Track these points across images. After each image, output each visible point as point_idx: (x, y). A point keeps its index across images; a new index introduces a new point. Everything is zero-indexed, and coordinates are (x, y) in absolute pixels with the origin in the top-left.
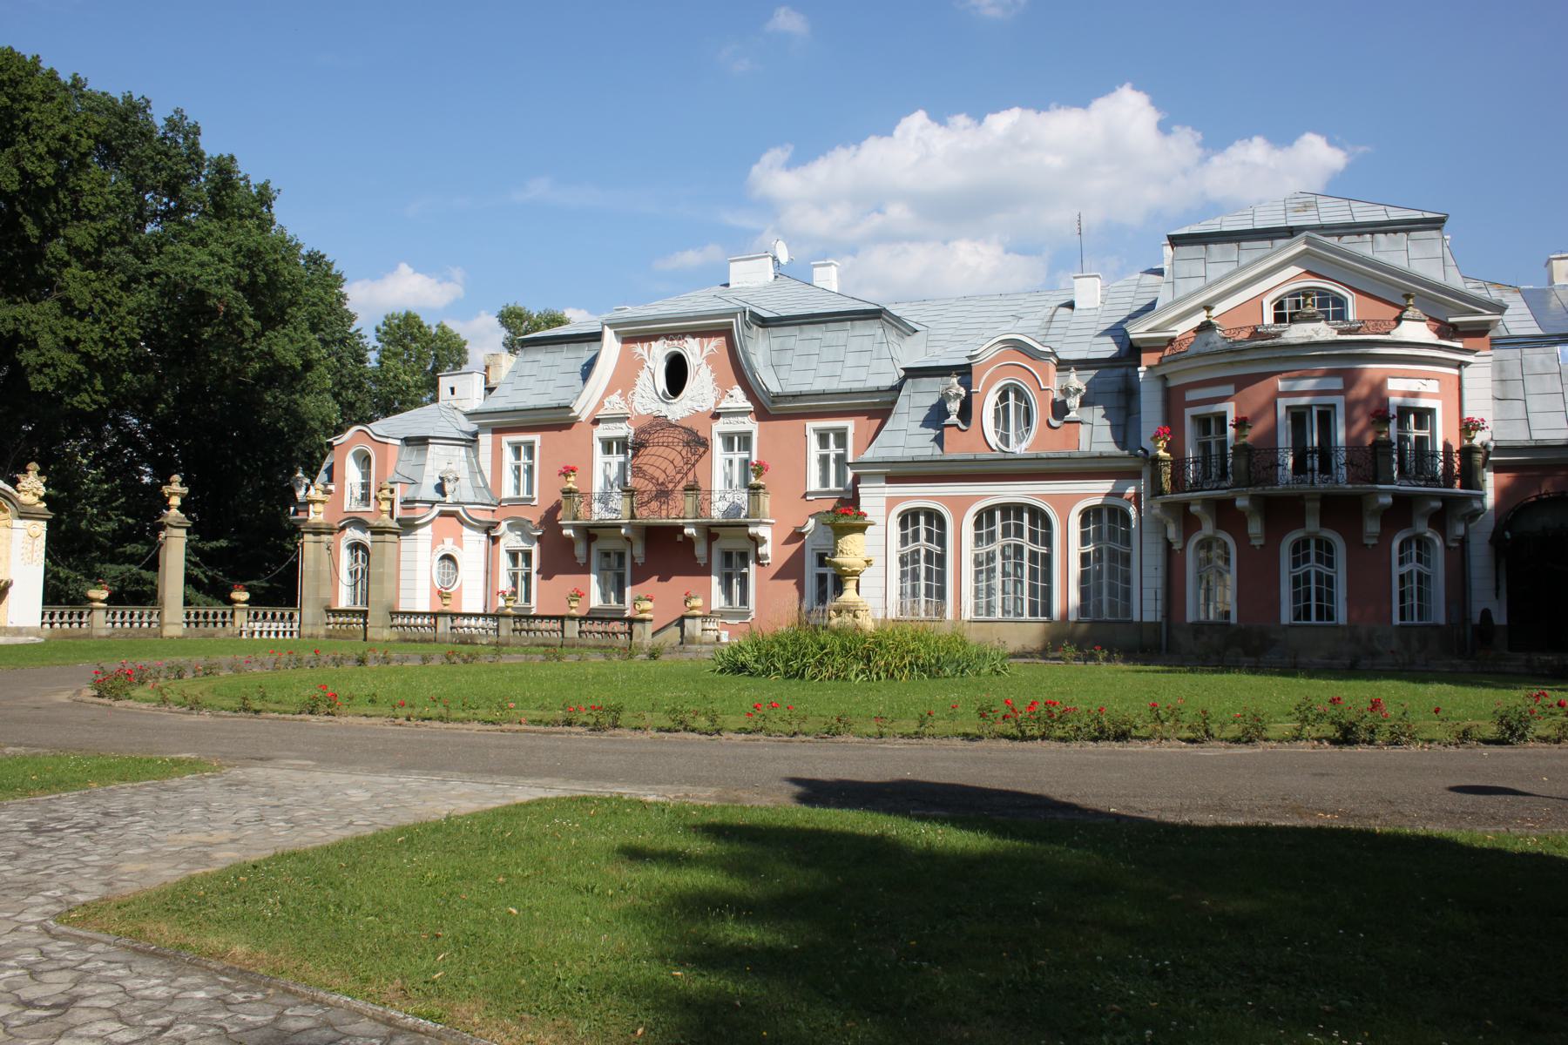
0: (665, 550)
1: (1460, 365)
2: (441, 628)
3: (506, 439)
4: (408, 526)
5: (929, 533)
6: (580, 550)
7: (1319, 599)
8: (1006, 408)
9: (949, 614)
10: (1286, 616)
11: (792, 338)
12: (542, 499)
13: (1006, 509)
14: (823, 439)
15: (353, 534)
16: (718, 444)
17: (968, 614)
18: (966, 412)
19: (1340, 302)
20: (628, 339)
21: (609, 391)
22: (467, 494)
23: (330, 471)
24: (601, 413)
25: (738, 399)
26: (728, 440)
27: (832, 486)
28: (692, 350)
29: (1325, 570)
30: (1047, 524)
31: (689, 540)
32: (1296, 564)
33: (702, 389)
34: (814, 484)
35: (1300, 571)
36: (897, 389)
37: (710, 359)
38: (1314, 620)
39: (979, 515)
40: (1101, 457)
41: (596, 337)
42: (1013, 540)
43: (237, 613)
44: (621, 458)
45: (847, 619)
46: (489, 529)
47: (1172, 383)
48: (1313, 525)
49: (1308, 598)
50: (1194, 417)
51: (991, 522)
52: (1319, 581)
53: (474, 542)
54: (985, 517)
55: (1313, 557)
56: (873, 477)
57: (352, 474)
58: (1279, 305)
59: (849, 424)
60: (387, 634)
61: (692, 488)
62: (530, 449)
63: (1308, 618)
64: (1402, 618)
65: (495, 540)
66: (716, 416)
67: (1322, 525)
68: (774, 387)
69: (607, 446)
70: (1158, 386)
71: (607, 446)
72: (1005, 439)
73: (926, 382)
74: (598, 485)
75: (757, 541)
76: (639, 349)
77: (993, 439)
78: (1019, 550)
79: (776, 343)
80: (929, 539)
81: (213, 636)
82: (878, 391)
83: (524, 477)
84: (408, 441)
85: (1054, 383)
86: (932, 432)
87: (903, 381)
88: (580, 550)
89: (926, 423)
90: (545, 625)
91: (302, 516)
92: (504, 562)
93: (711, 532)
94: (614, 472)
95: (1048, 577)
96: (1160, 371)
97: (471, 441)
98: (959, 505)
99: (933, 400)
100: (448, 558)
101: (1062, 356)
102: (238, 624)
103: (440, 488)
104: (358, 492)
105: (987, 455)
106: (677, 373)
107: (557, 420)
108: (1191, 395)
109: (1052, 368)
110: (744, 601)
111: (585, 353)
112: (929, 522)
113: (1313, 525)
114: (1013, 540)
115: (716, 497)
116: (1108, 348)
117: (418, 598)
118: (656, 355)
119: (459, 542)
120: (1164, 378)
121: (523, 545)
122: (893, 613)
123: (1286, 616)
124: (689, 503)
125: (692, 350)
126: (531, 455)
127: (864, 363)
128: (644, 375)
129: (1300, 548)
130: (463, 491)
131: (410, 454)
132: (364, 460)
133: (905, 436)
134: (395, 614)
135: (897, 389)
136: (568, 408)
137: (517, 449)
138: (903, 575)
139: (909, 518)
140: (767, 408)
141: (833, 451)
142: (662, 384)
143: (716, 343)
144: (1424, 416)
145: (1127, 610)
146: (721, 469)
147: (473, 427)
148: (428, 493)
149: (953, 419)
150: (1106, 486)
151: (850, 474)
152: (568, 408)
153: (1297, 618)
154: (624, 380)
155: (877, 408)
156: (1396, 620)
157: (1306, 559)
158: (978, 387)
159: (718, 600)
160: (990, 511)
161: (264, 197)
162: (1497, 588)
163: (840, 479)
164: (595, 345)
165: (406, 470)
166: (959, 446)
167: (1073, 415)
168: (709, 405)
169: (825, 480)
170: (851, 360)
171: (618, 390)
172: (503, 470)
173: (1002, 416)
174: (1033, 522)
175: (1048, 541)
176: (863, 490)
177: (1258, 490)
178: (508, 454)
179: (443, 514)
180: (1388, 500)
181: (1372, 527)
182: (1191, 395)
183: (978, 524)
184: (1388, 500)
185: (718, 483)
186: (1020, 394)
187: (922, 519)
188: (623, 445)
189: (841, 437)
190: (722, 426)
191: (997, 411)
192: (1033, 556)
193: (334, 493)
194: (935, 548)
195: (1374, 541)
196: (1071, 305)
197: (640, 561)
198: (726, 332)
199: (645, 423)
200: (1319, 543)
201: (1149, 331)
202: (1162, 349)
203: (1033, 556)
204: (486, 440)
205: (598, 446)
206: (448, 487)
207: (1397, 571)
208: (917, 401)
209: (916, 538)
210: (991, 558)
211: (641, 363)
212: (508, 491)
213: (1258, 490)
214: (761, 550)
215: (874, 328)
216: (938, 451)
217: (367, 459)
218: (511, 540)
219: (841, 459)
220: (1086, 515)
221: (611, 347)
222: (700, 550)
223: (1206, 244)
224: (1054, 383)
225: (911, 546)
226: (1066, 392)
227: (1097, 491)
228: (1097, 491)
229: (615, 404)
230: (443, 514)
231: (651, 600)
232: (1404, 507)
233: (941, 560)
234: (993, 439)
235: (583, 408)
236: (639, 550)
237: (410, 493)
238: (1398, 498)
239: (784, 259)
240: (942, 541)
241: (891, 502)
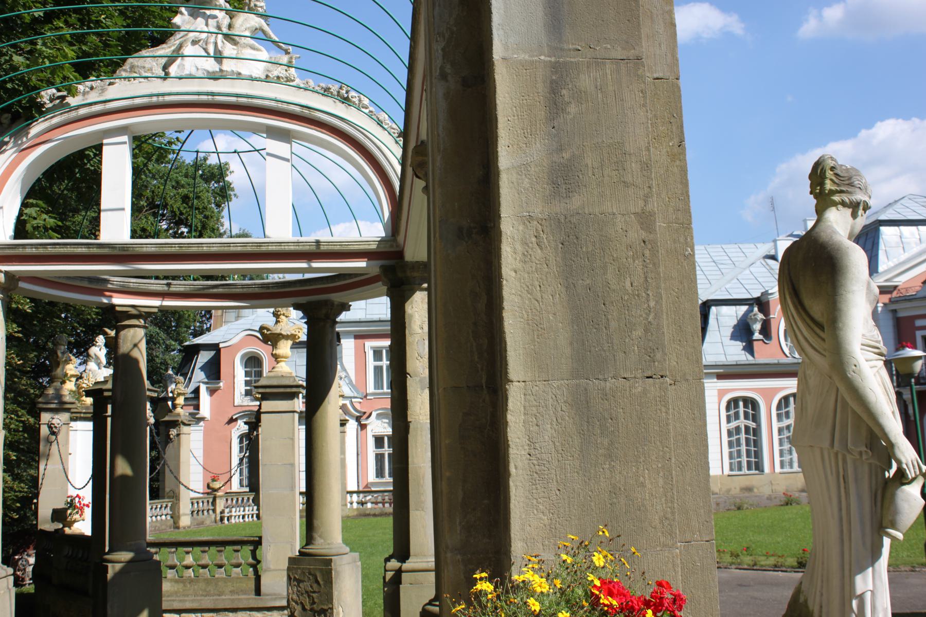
3: (370, 344)
9: (767, 468)
17: (778, 469)
18: (766, 331)
39: (780, 401)
43: (218, 501)
47: (901, 314)
56: (709, 375)
70: (890, 315)
73: (725, 309)
80: (746, 417)
81: (202, 523)
86: (739, 345)
89: (734, 337)
95: (757, 443)
96: (894, 307)
98: (768, 394)
102: (218, 510)
105: (784, 360)
120: (894, 312)
138: (730, 444)
149: (757, 336)
160: (786, 399)
182: (919, 323)
187: (741, 404)
194: (752, 425)
201: (886, 281)
202: (890, 292)
209: (737, 416)
216: (750, 357)
223: (898, 225)
225: (734, 424)
233: (757, 432)
241: (722, 393)
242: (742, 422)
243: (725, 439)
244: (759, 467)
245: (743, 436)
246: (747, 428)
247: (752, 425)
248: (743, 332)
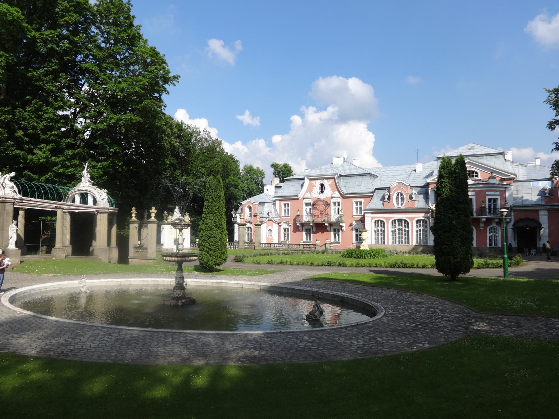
0: (320, 228)
1: (505, 188)
3: (283, 203)
4: (262, 223)
6: (300, 228)
8: (398, 198)
11: (349, 179)
12: (291, 217)
13: (398, 220)
14: (356, 203)
15: (248, 225)
16: (332, 204)
18: (389, 198)
19: (477, 173)
20: (311, 180)
21: (306, 192)
22: (274, 216)
23: (242, 209)
24: (305, 197)
25: (337, 194)
26: (334, 203)
27: (359, 214)
28: (325, 182)
30: (408, 223)
31: (326, 226)
33: (328, 192)
34: (354, 213)
36: (373, 192)
37: (330, 185)
40: (420, 209)
41: (303, 179)
42: (400, 227)
44: (310, 207)
46: (279, 223)
51: (395, 223)
53: (276, 226)
54: (394, 222)
57: (247, 210)
59: (362, 200)
60: (259, 248)
61: (327, 215)
62: (288, 205)
64: (490, 245)
65: (280, 226)
66: (332, 198)
68: (345, 192)
69: (306, 204)
71: (306, 204)
72: (398, 204)
74: (304, 214)
75: (342, 227)
76: (313, 182)
77: (396, 205)
78: (401, 229)
79: (345, 181)
82: (369, 193)
83: (287, 211)
84: (259, 203)
85: (410, 191)
86: (382, 202)
87: (375, 190)
88: (300, 228)
90: (295, 246)
91: (235, 220)
92: (283, 231)
93: (331, 224)
94: (308, 211)
97: (274, 203)
98: (388, 219)
99: (381, 195)
100: (270, 230)
101: (411, 185)
103: (268, 214)
104: (249, 215)
106: (322, 188)
107: (294, 198)
109: (409, 188)
110: (339, 240)
111: (301, 182)
112: (381, 223)
114: (400, 227)
115: (332, 217)
116: (423, 184)
117: (264, 240)
118: (318, 183)
119: (272, 227)
121: (287, 227)
122: (373, 243)
124: (326, 218)
125: (325, 182)
126: (288, 206)
127: (366, 186)
128: (315, 188)
130: (273, 215)
131: (260, 207)
132: (250, 208)
133: (376, 203)
134: (260, 244)
135: (373, 192)
136: (297, 196)
137: (285, 205)
139: (376, 222)
140: (343, 196)
141: (359, 206)
142: (319, 191)
143: (331, 181)
144: (495, 200)
145: (427, 243)
146: (333, 209)
147: (274, 199)
148: (265, 215)
149: (386, 200)
150: (423, 215)
151: (363, 212)
152: (297, 196)
154: (310, 189)
155: (370, 196)
156: (488, 246)
158: (392, 193)
159: (333, 239)
160: (395, 221)
162: (514, 239)
163: (361, 213)
164: (303, 181)
165: (259, 210)
166: (388, 206)
167: (414, 199)
168: (330, 195)
170: (363, 185)
171: (309, 192)
172: (281, 208)
173: (397, 199)
174: (405, 223)
175: (408, 227)
176: (366, 215)
178: (283, 206)
179: (269, 220)
180: (485, 220)
181: (482, 225)
183: (392, 223)
184: (485, 220)
185: (332, 213)
186: (402, 195)
188: (310, 204)
189: (361, 203)
190: (333, 200)
192: (405, 231)
193: (242, 216)
194: (383, 229)
196: (415, 171)
198: (334, 178)
199: (315, 200)
203: (405, 231)
204: (277, 202)
205: (304, 205)
206: (270, 214)
207: (488, 235)
208: (378, 195)
209: (378, 226)
210: (395, 231)
211: (314, 186)
212: (283, 215)
214: (343, 228)
215: (368, 178)
218: (284, 226)
219: (361, 208)
220: (417, 222)
221: (307, 181)
222: (329, 228)
224: (410, 191)
226: (412, 194)
227: (421, 216)
228: (421, 216)
229: (308, 195)
230: (269, 220)
231: (318, 239)
232: (489, 221)
233: (384, 231)
234: (396, 205)
235: (300, 196)
236: (314, 228)
237: (261, 216)
238: (486, 219)
239: (346, 157)
240: (384, 227)
241: (372, 218)
242: (380, 228)
244: (384, 243)
247: (383, 229)
248: (383, 199)
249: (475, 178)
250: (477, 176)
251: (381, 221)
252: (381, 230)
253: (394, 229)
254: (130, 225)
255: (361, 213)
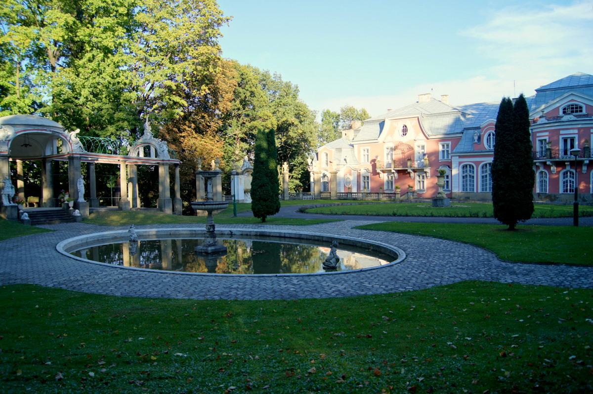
2: (348, 196)
3: (361, 148)
5: (470, 170)
7: (570, 187)
8: (490, 138)
9: (475, 191)
10: (561, 191)
18: (479, 138)
19: (581, 107)
29: (572, 179)
32: (564, 178)
35: (565, 180)
38: (569, 192)
45: (440, 195)
48: (568, 168)
49: (567, 187)
50: (539, 140)
52: (570, 182)
55: (569, 176)
58: (565, 109)
59: (450, 143)
63: (567, 191)
67: (571, 168)
82: (457, 133)
98: (477, 163)
106: (405, 130)
108: (538, 135)
112: (470, 167)
113: (568, 168)
122: (460, 191)
123: (561, 191)
129: (565, 174)
139: (465, 167)
142: (402, 133)
153: (564, 192)
157: (567, 177)
161: (297, 90)
163: (448, 157)
169: (443, 157)
177: (552, 160)
181: (584, 168)
182: (538, 135)
191: (487, 139)
195: (584, 172)
197: (396, 178)
200: (570, 172)
209: (467, 171)
210: (486, 176)
213: (552, 160)
217: (327, 154)
219: (448, 151)
225: (465, 174)
240: (473, 172)
241: (460, 163)
243: (461, 178)
244: (473, 190)
245: (468, 178)
246: (470, 176)
247: (471, 174)
249: (579, 113)
250: (581, 111)
251: (470, 165)
252: (470, 176)
253: (484, 175)
254: (197, 176)
255: (448, 157)
